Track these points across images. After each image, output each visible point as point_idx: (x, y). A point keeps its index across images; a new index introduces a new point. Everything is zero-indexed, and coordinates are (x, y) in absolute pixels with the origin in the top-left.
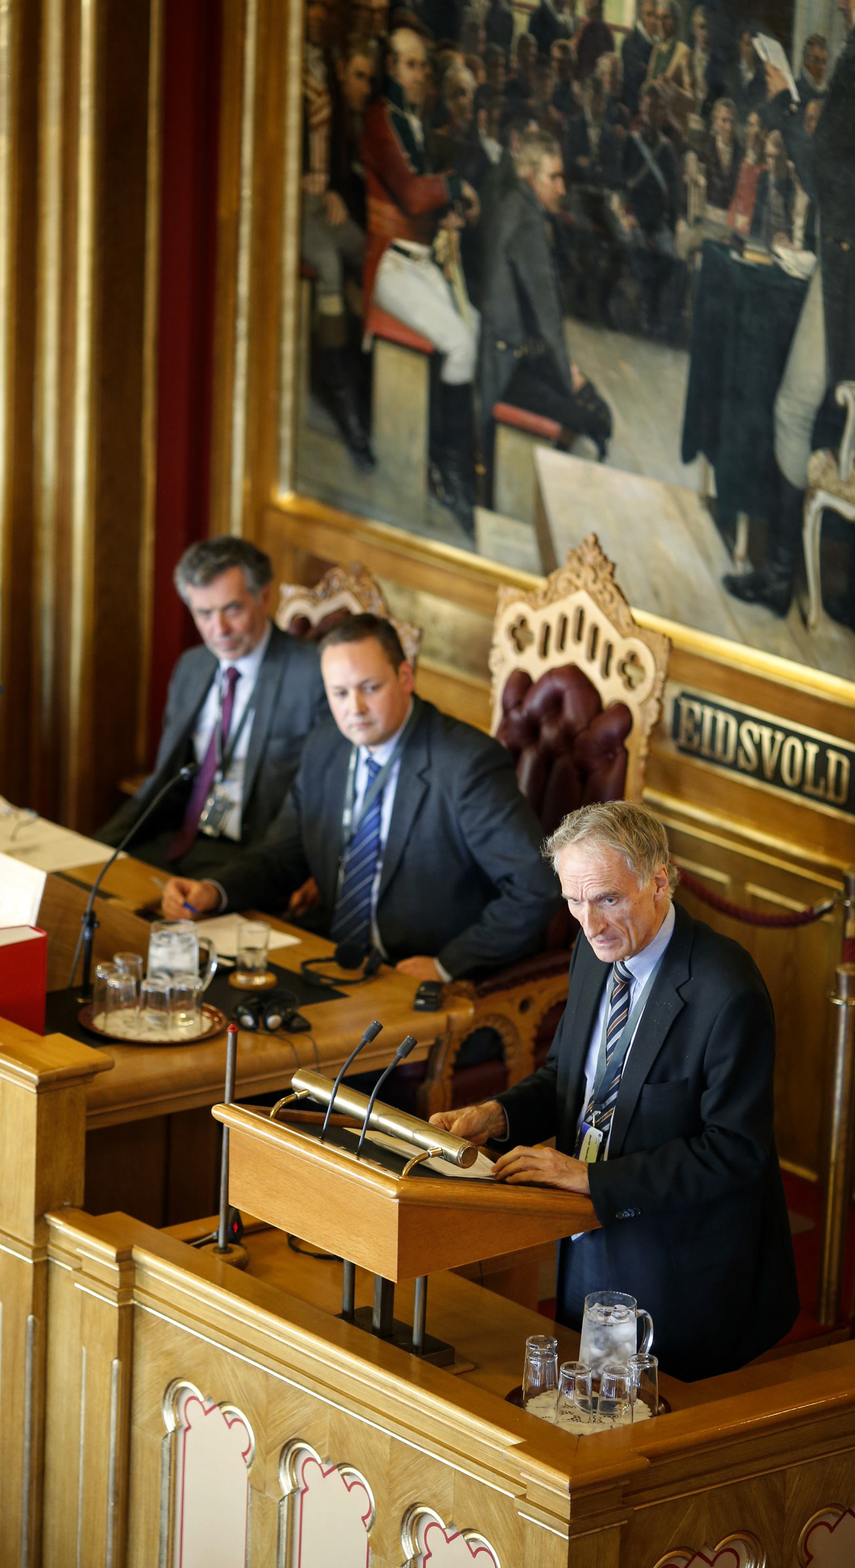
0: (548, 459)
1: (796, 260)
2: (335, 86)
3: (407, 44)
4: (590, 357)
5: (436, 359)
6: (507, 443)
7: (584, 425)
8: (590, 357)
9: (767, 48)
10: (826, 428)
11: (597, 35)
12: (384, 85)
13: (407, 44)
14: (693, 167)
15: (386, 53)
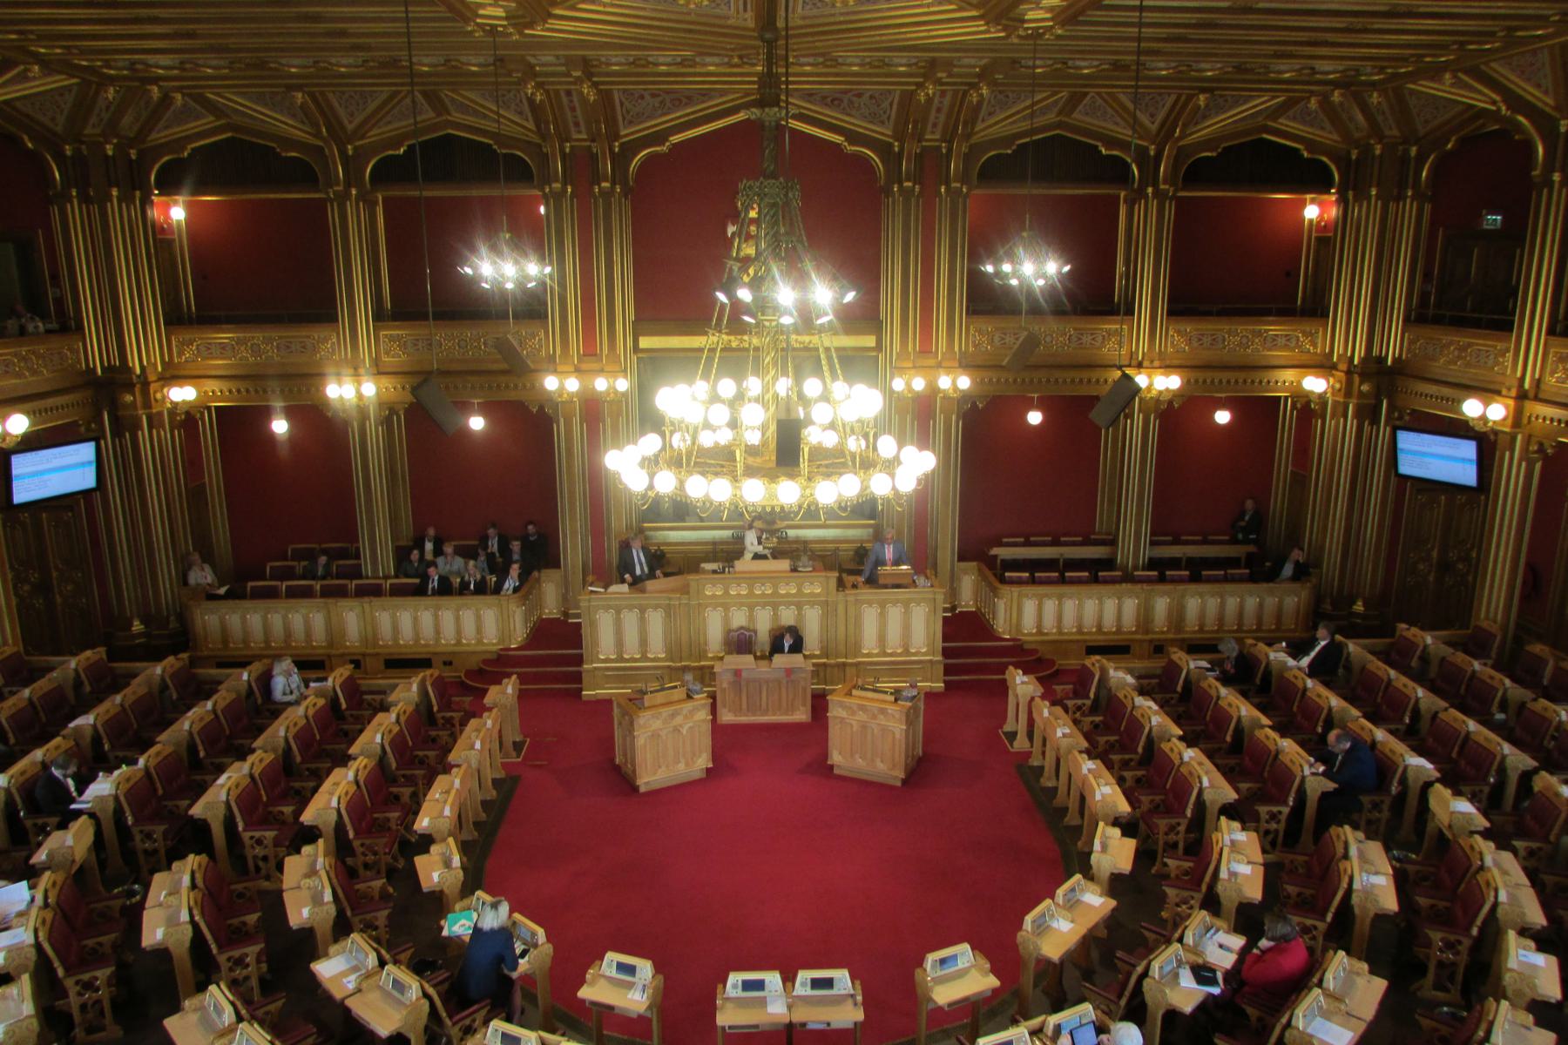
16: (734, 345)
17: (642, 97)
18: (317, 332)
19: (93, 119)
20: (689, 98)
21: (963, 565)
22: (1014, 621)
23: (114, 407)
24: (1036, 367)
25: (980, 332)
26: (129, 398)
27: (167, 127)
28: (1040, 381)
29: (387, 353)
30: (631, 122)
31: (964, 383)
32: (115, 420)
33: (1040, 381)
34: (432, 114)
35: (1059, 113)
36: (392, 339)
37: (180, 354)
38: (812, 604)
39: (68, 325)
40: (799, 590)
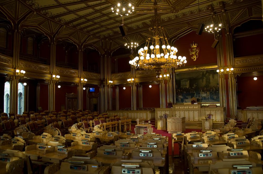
0: (186, 100)
1: (194, 92)
2: (176, 92)
3: (179, 90)
4: (187, 97)
5: (181, 98)
6: (184, 100)
7: (187, 98)
8: (187, 97)
9: (193, 87)
10: (196, 96)
11: (187, 88)
12: (178, 91)
13: (179, 90)
14: (191, 91)
15: (178, 91)
16: (191, 70)
17: (170, 29)
18: (128, 73)
19: (103, 46)
20: (179, 29)
21: (239, 110)
22: (246, 118)
23: (103, 83)
24: (251, 66)
25: (237, 61)
26: (104, 82)
27: (113, 47)
28: (252, 69)
29: (137, 75)
30: (170, 34)
31: (232, 69)
32: (103, 85)
33: (252, 69)
34: (143, 39)
35: (249, 16)
36: (138, 73)
37: (112, 77)
38: (196, 110)
39: (100, 73)
40: (193, 108)
